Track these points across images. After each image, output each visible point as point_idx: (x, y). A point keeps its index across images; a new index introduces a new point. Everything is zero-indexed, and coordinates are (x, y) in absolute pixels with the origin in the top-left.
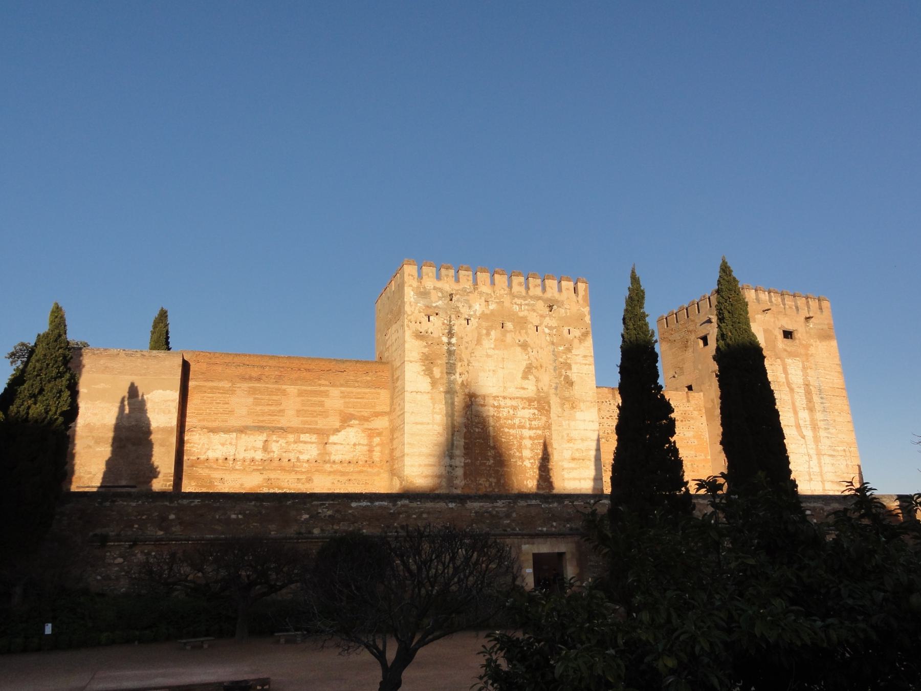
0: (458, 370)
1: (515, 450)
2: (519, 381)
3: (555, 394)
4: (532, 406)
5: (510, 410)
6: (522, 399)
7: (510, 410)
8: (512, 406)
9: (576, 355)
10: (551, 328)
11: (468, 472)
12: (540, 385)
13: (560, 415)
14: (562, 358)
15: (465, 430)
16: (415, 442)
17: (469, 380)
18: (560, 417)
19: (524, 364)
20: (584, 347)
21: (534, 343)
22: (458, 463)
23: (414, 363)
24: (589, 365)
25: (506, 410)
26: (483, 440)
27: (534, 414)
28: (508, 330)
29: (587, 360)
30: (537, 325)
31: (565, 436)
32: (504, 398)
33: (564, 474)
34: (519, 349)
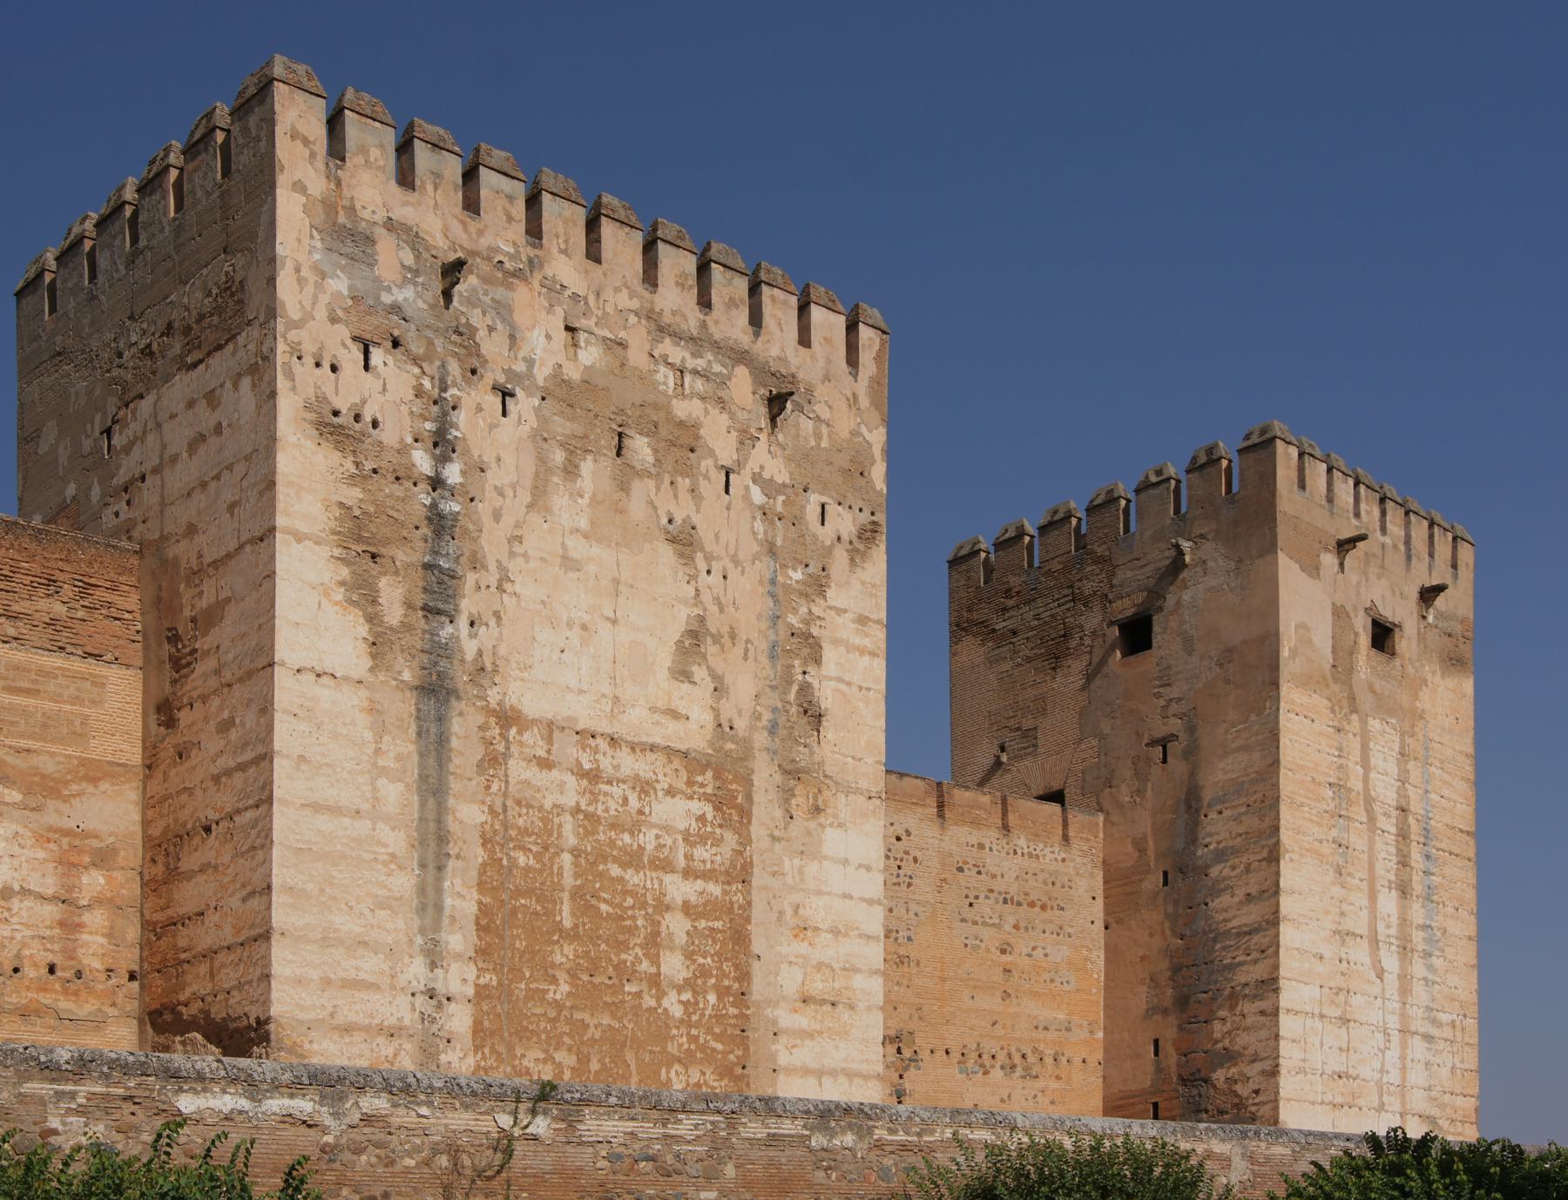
0: (468, 605)
1: (638, 950)
2: (661, 685)
3: (767, 749)
4: (696, 788)
5: (629, 793)
6: (670, 752)
7: (629, 793)
8: (637, 778)
9: (840, 611)
10: (769, 487)
11: (486, 1023)
12: (727, 710)
13: (777, 833)
14: (795, 611)
15: (481, 855)
16: (310, 887)
17: (502, 651)
18: (779, 839)
19: (681, 618)
20: (863, 583)
21: (717, 535)
22: (455, 987)
23: (309, 543)
24: (873, 654)
25: (617, 791)
26: (538, 901)
27: (701, 819)
28: (639, 467)
29: (867, 635)
30: (728, 463)
31: (789, 912)
32: (613, 741)
33: (777, 1051)
34: (666, 552)
